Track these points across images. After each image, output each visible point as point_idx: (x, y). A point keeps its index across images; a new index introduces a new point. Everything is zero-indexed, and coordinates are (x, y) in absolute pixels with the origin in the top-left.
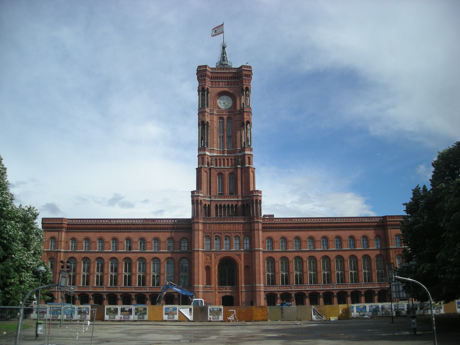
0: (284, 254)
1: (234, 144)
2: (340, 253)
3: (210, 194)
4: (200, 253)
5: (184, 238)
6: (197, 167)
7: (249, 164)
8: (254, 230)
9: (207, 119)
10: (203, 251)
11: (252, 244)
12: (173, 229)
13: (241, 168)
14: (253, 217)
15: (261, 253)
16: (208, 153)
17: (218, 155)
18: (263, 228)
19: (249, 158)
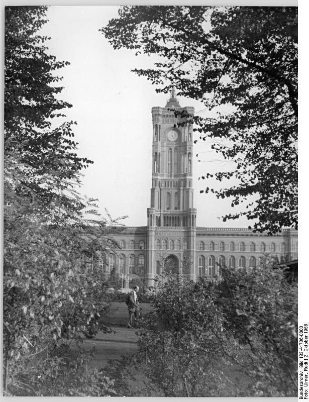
0: (212, 254)
1: (179, 169)
2: (253, 255)
3: (161, 209)
4: (153, 252)
5: (140, 241)
6: (151, 188)
7: (190, 186)
8: (190, 236)
9: (159, 150)
10: (155, 251)
11: (188, 247)
12: (136, 234)
13: (183, 190)
14: (190, 228)
15: (195, 253)
16: (159, 177)
17: (167, 178)
18: (197, 235)
19: (190, 182)
